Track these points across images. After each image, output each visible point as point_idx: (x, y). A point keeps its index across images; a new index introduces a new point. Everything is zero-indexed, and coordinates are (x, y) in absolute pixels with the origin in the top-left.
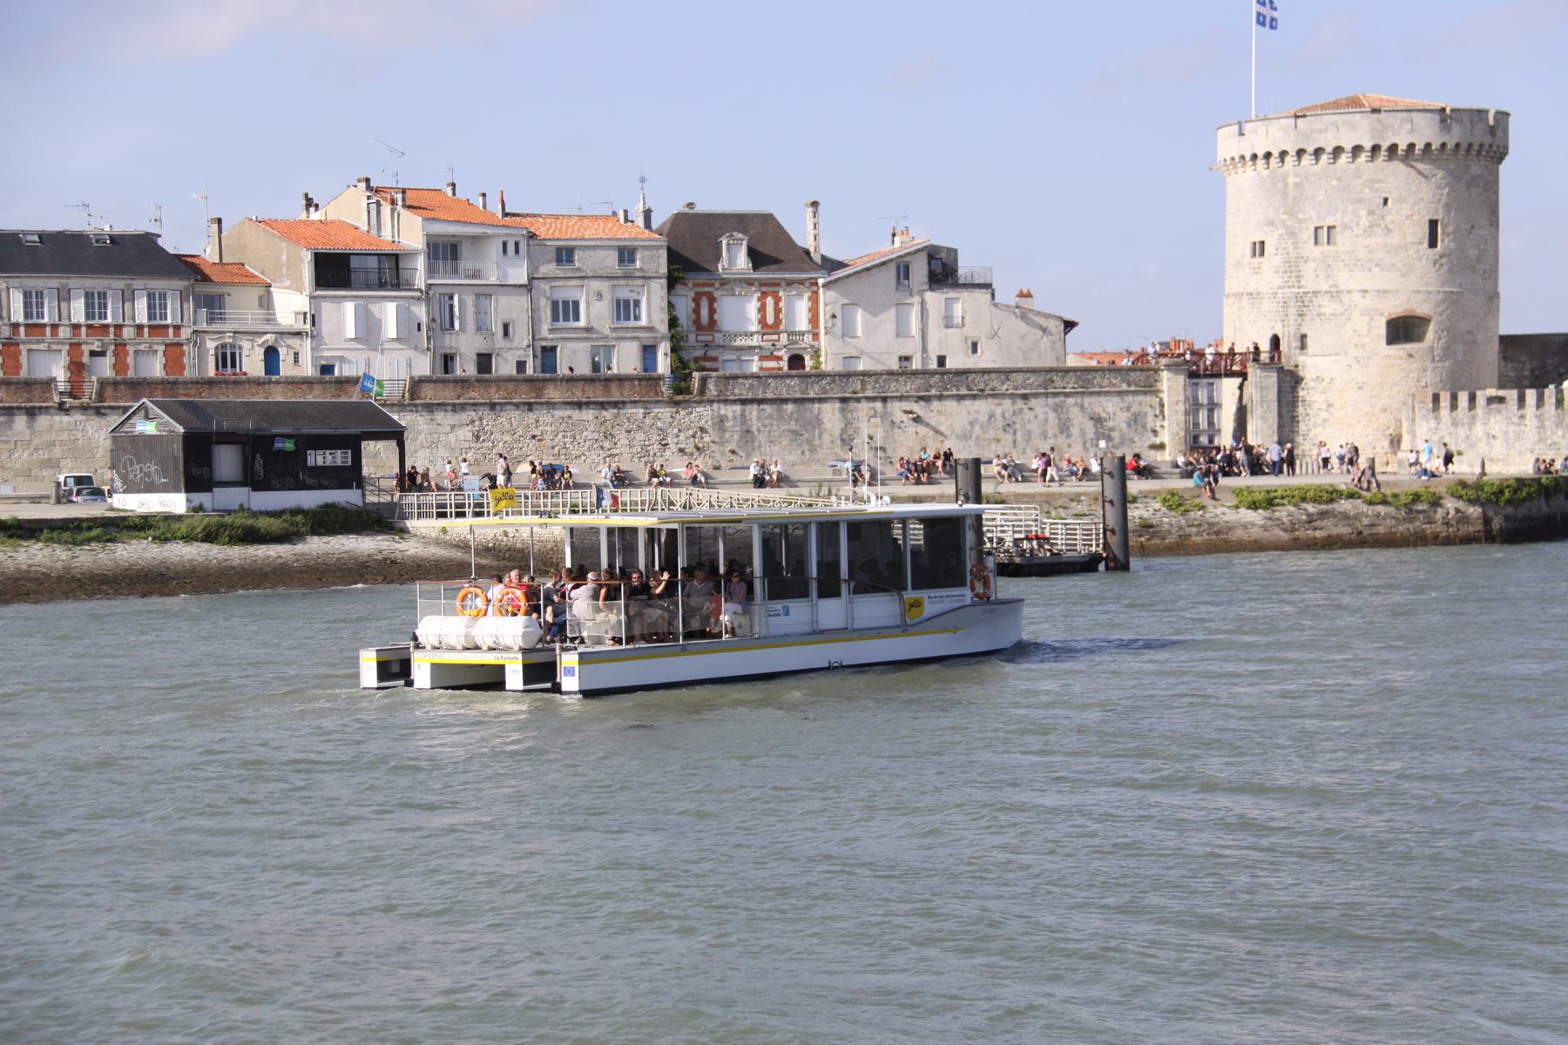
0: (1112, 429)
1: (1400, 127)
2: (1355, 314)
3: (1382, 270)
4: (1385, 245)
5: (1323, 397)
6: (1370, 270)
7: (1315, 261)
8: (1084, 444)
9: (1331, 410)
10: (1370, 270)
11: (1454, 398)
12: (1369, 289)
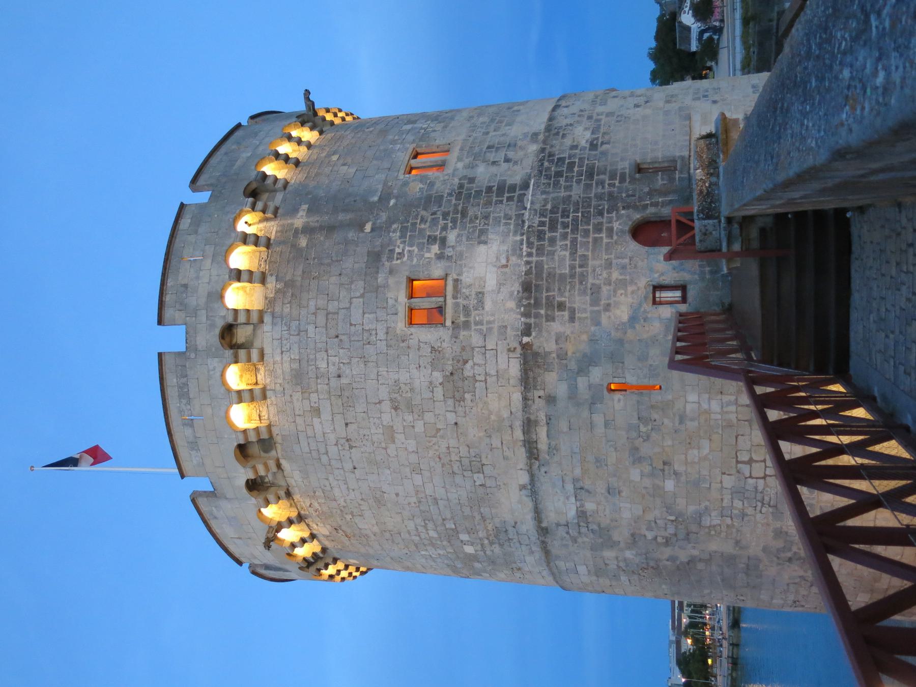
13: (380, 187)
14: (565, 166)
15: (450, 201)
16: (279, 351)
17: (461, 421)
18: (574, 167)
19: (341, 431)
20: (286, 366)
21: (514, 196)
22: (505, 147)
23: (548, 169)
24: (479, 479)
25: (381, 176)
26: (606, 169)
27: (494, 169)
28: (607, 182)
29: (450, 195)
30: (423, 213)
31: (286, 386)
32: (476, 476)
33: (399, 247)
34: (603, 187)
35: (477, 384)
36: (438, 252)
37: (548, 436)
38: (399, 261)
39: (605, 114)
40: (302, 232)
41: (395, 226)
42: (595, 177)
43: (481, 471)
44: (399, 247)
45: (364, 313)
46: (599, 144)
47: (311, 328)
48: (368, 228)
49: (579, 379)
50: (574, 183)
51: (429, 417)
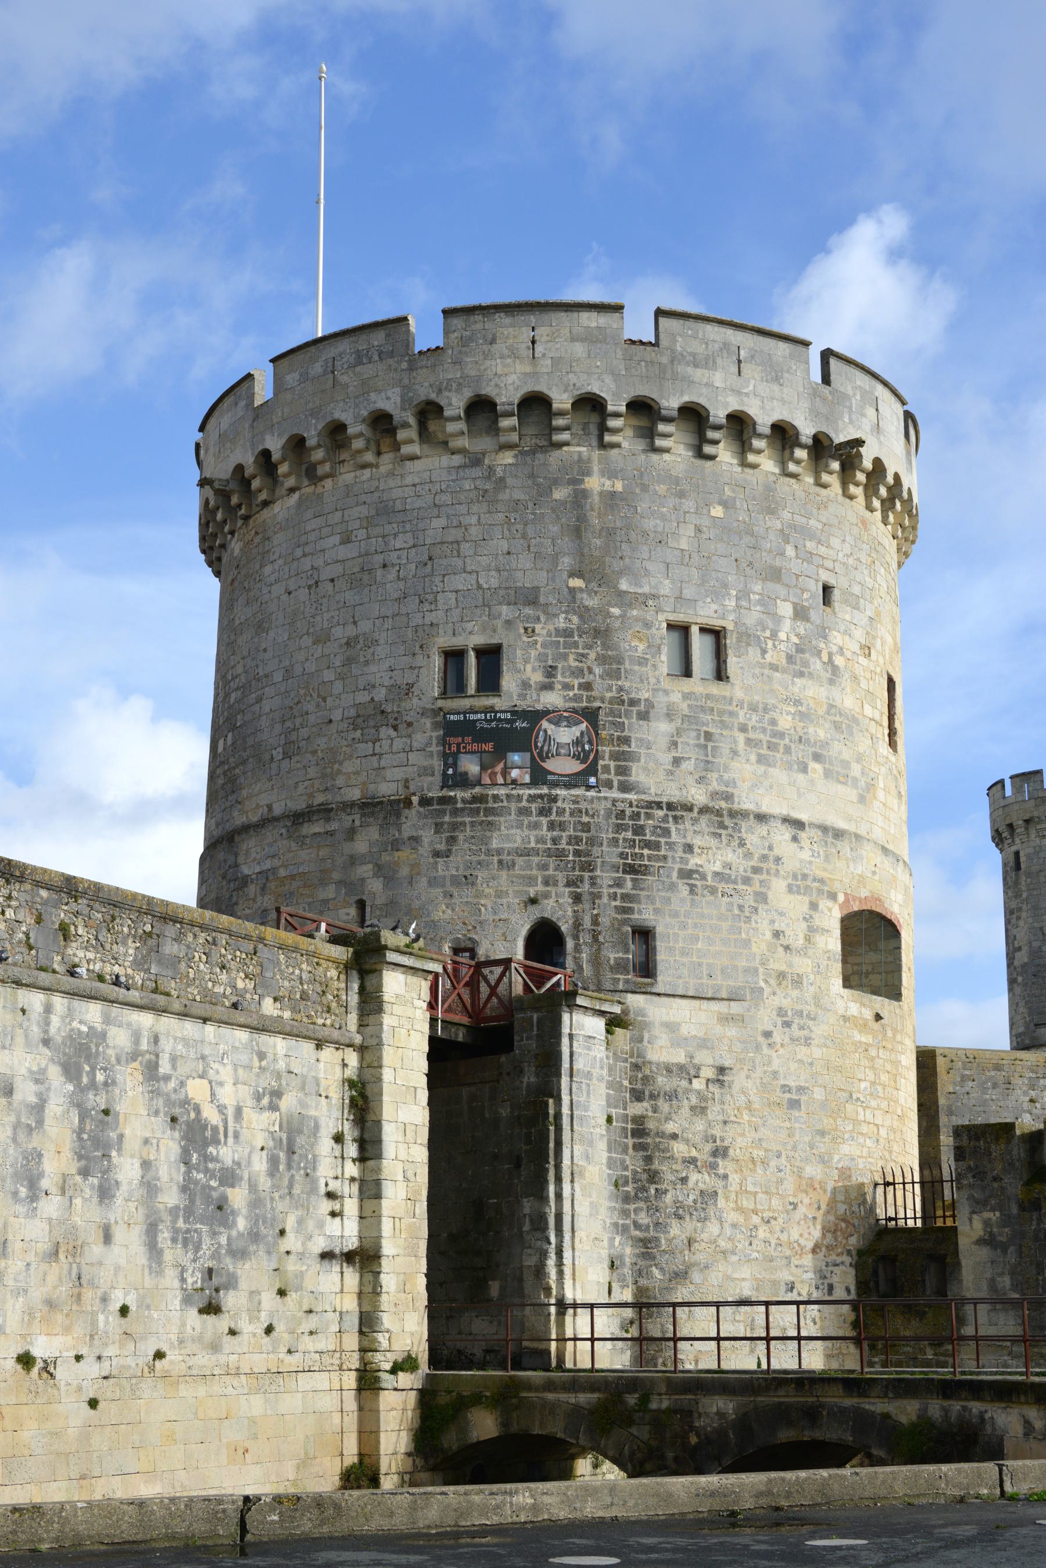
0: (229, 1177)
2: (778, 886)
5: (700, 1125)
6: (804, 769)
7: (669, 716)
8: (152, 1230)
9: (722, 1164)
10: (804, 769)
13: (646, 589)
14: (653, 838)
15: (610, 689)
16: (417, 480)
17: (333, 727)
18: (650, 849)
19: (326, 574)
20: (397, 493)
21: (610, 773)
22: (707, 756)
23: (649, 816)
24: (278, 754)
25: (666, 588)
26: (642, 889)
27: (663, 742)
28: (619, 891)
29: (621, 689)
30: (592, 655)
31: (376, 494)
32: (280, 749)
33: (543, 628)
34: (610, 886)
35: (370, 744)
36: (532, 683)
37: (315, 834)
38: (522, 631)
39: (764, 890)
40: (575, 491)
41: (575, 619)
42: (628, 877)
43: (287, 756)
44: (543, 628)
45: (456, 592)
46: (693, 882)
47: (442, 522)
48: (576, 583)
49: (370, 866)
50: (620, 850)
51: (338, 686)
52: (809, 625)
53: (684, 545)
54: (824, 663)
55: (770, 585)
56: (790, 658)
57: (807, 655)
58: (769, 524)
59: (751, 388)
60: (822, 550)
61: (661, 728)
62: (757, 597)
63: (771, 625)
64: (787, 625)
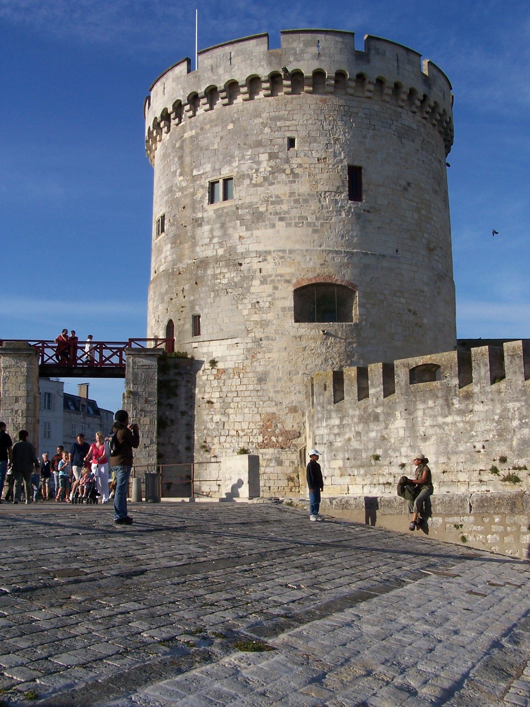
1: (302, 52)
3: (288, 225)
4: (292, 194)
6: (273, 226)
7: (208, 223)
10: (273, 226)
11: (363, 374)
12: (272, 249)
13: (202, 172)
52: (279, 160)
53: (216, 147)
54: (287, 175)
55: (257, 149)
56: (265, 179)
57: (276, 174)
58: (256, 122)
59: (236, 67)
60: (288, 123)
61: (206, 228)
62: (248, 157)
63: (255, 166)
64: (264, 164)
